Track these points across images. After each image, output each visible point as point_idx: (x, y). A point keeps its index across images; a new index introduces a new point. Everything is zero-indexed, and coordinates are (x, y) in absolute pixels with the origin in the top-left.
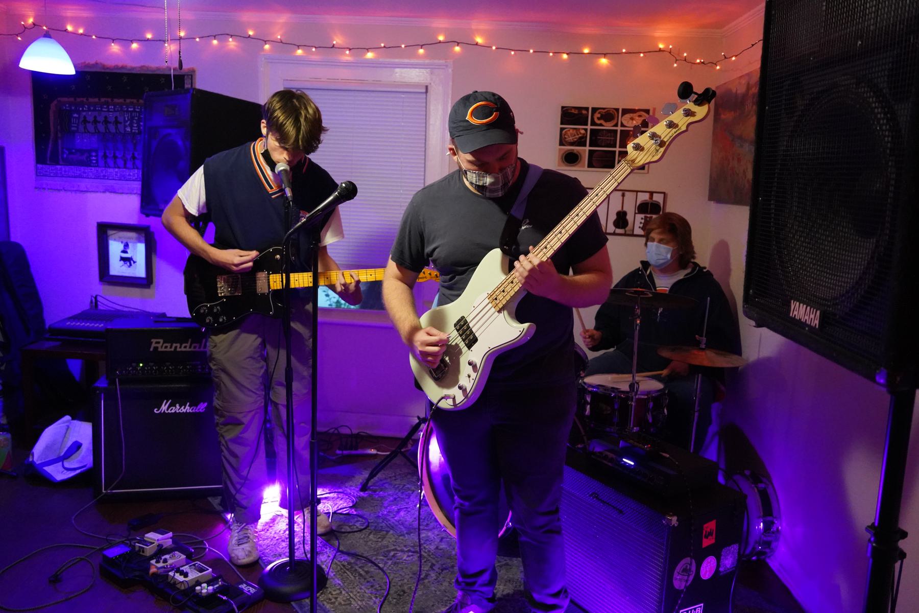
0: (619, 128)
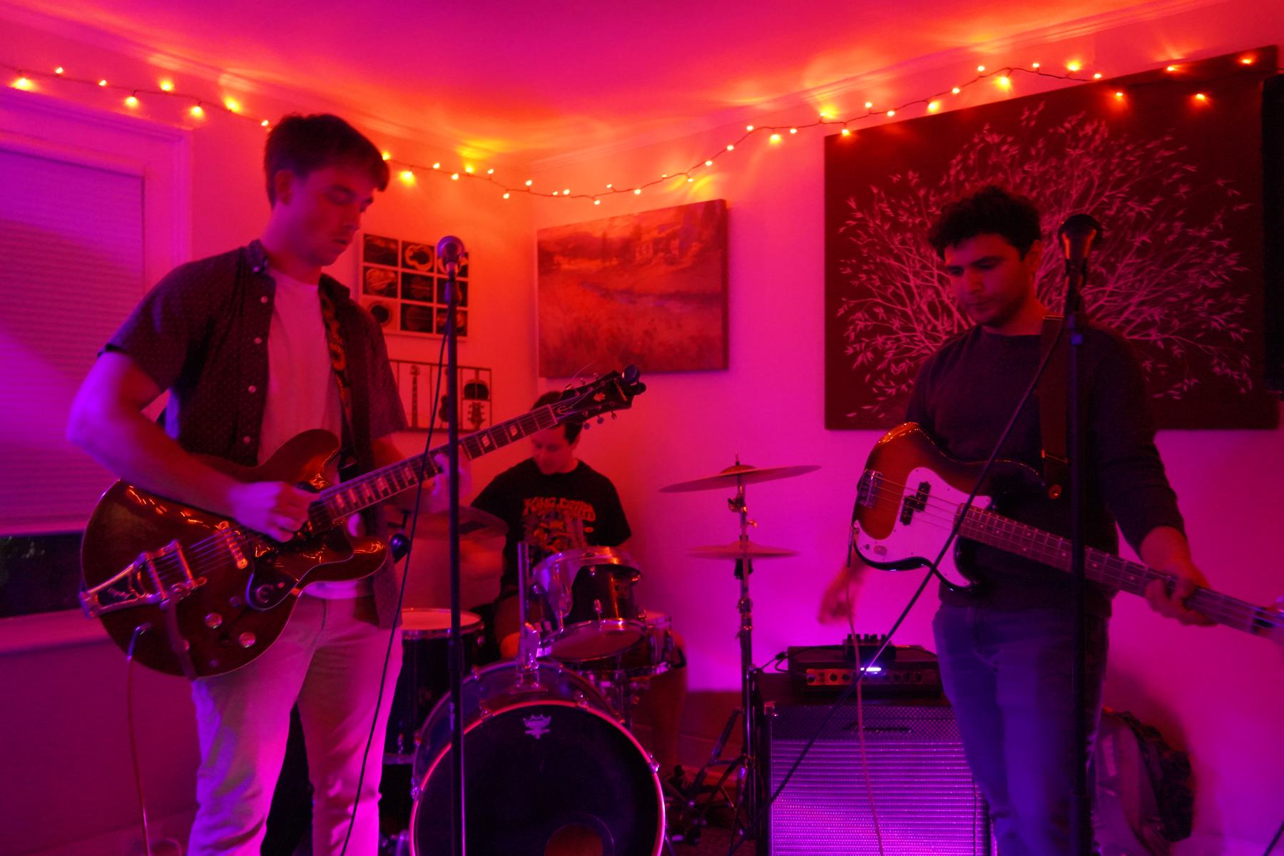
0: (435, 275)
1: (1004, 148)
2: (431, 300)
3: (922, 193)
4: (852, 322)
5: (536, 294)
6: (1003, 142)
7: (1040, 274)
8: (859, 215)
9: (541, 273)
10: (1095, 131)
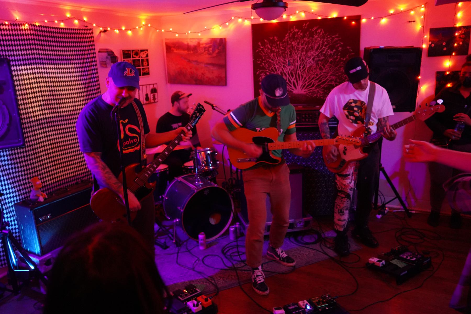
0: (140, 58)
1: (299, 33)
2: (140, 66)
3: (278, 43)
4: (261, 76)
5: (166, 61)
6: (299, 32)
7: (308, 66)
8: (262, 47)
9: (167, 52)
10: (321, 31)
